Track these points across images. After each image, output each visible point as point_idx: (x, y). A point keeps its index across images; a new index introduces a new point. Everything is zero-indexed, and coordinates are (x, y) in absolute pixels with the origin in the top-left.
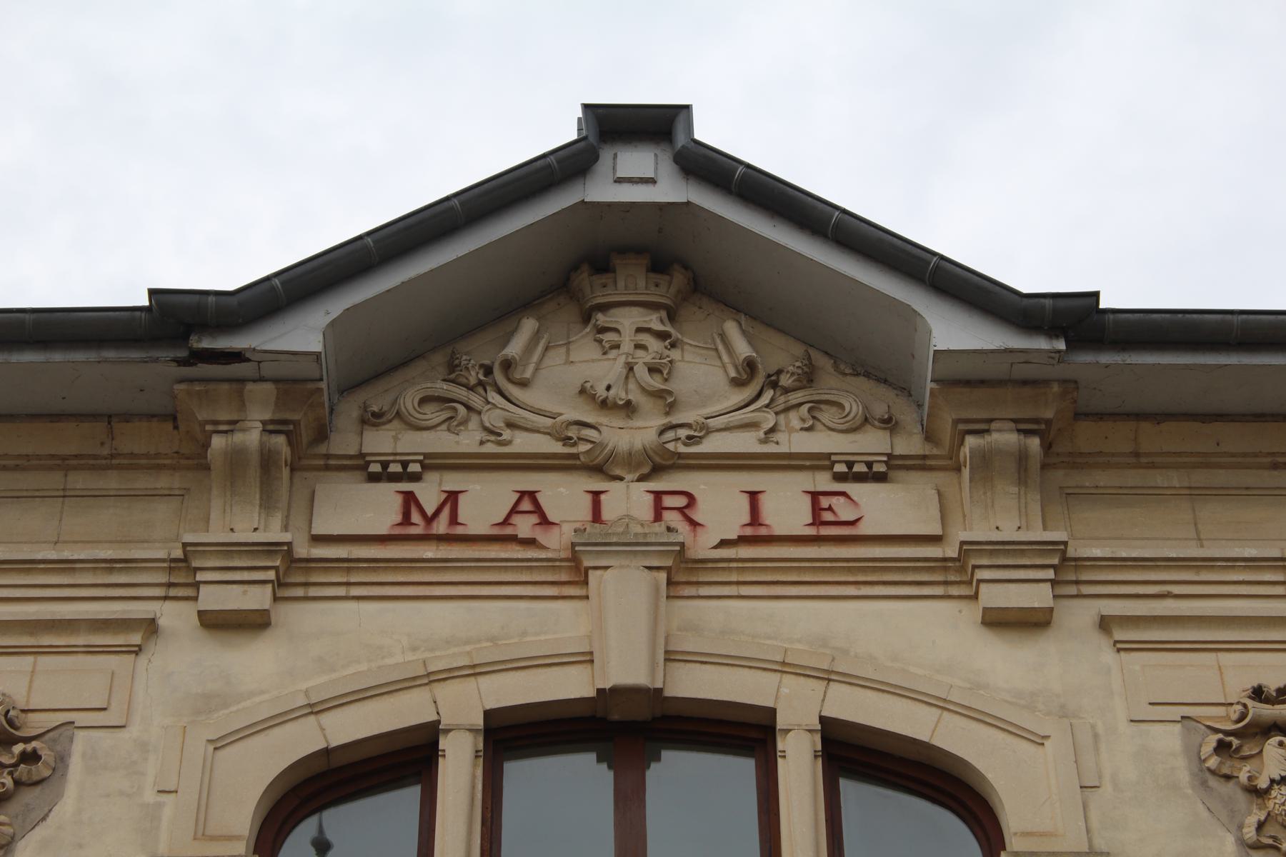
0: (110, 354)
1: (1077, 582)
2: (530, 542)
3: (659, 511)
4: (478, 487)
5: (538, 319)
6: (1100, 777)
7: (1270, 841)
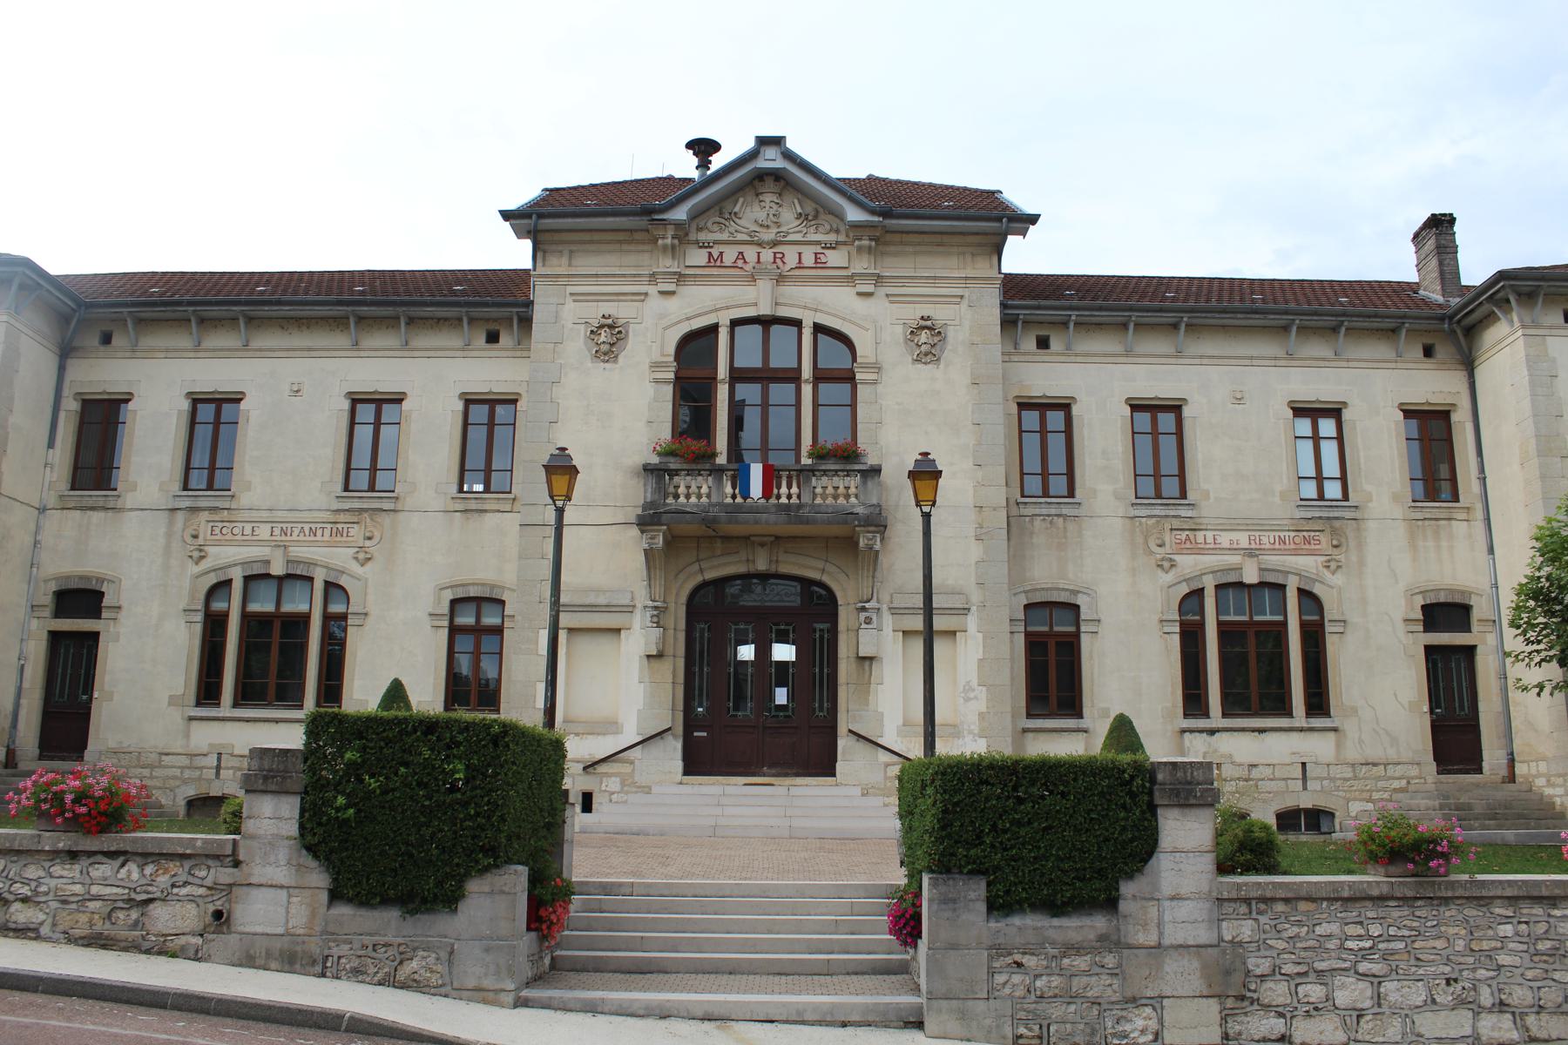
3: (775, 258)
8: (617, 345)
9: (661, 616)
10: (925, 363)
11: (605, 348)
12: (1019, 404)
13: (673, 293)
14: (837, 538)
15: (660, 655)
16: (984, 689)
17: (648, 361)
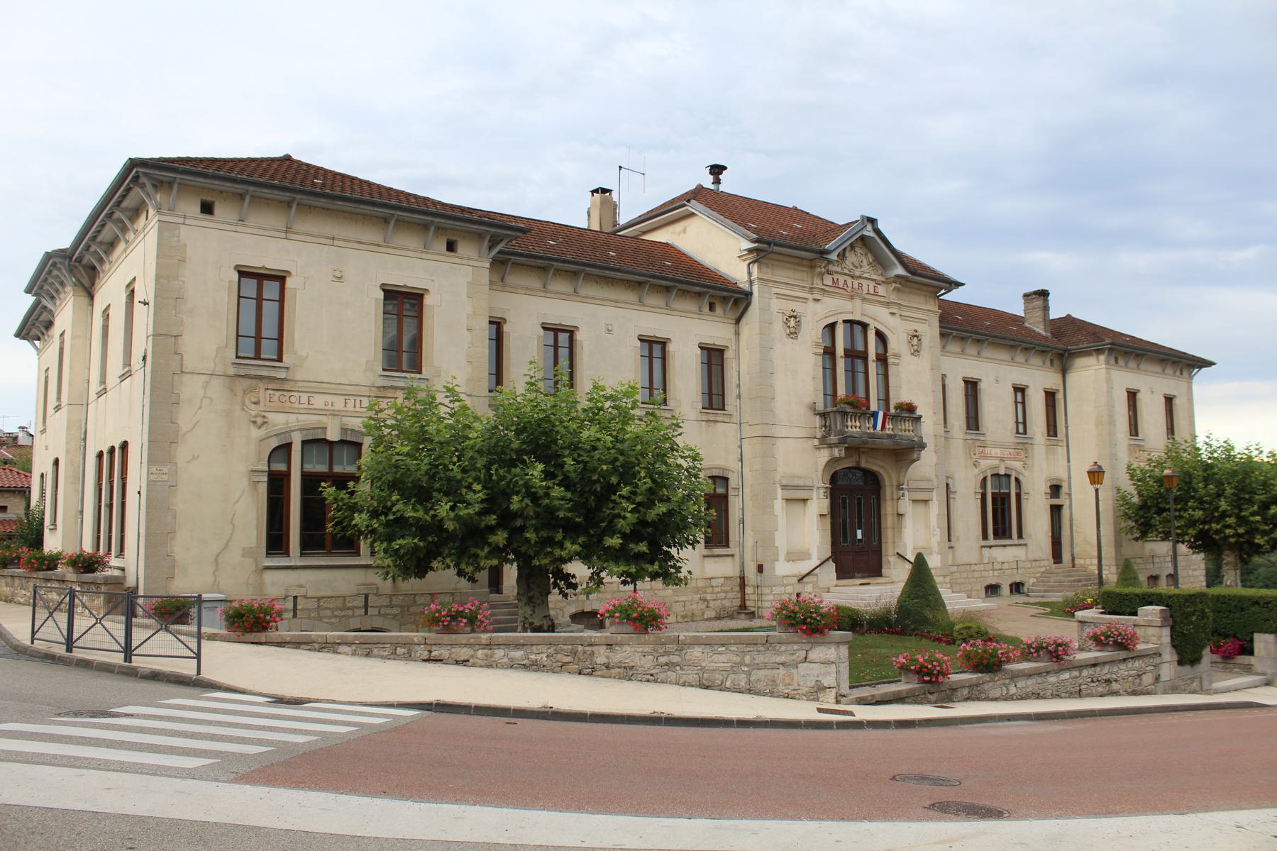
11: (793, 330)
12: (240, 272)
13: (818, 300)
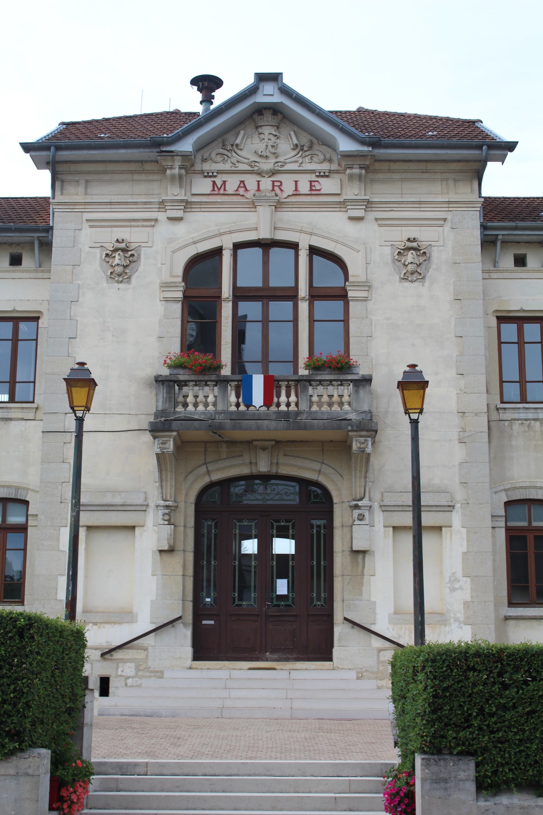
0: (142, 150)
1: (371, 207)
2: (243, 196)
3: (273, 186)
4: (230, 180)
5: (244, 130)
6: (371, 261)
7: (407, 278)
8: (130, 267)
9: (172, 514)
10: (412, 281)
11: (119, 269)
13: (180, 219)
14: (331, 441)
15: (171, 550)
16: (468, 580)
17: (158, 281)
